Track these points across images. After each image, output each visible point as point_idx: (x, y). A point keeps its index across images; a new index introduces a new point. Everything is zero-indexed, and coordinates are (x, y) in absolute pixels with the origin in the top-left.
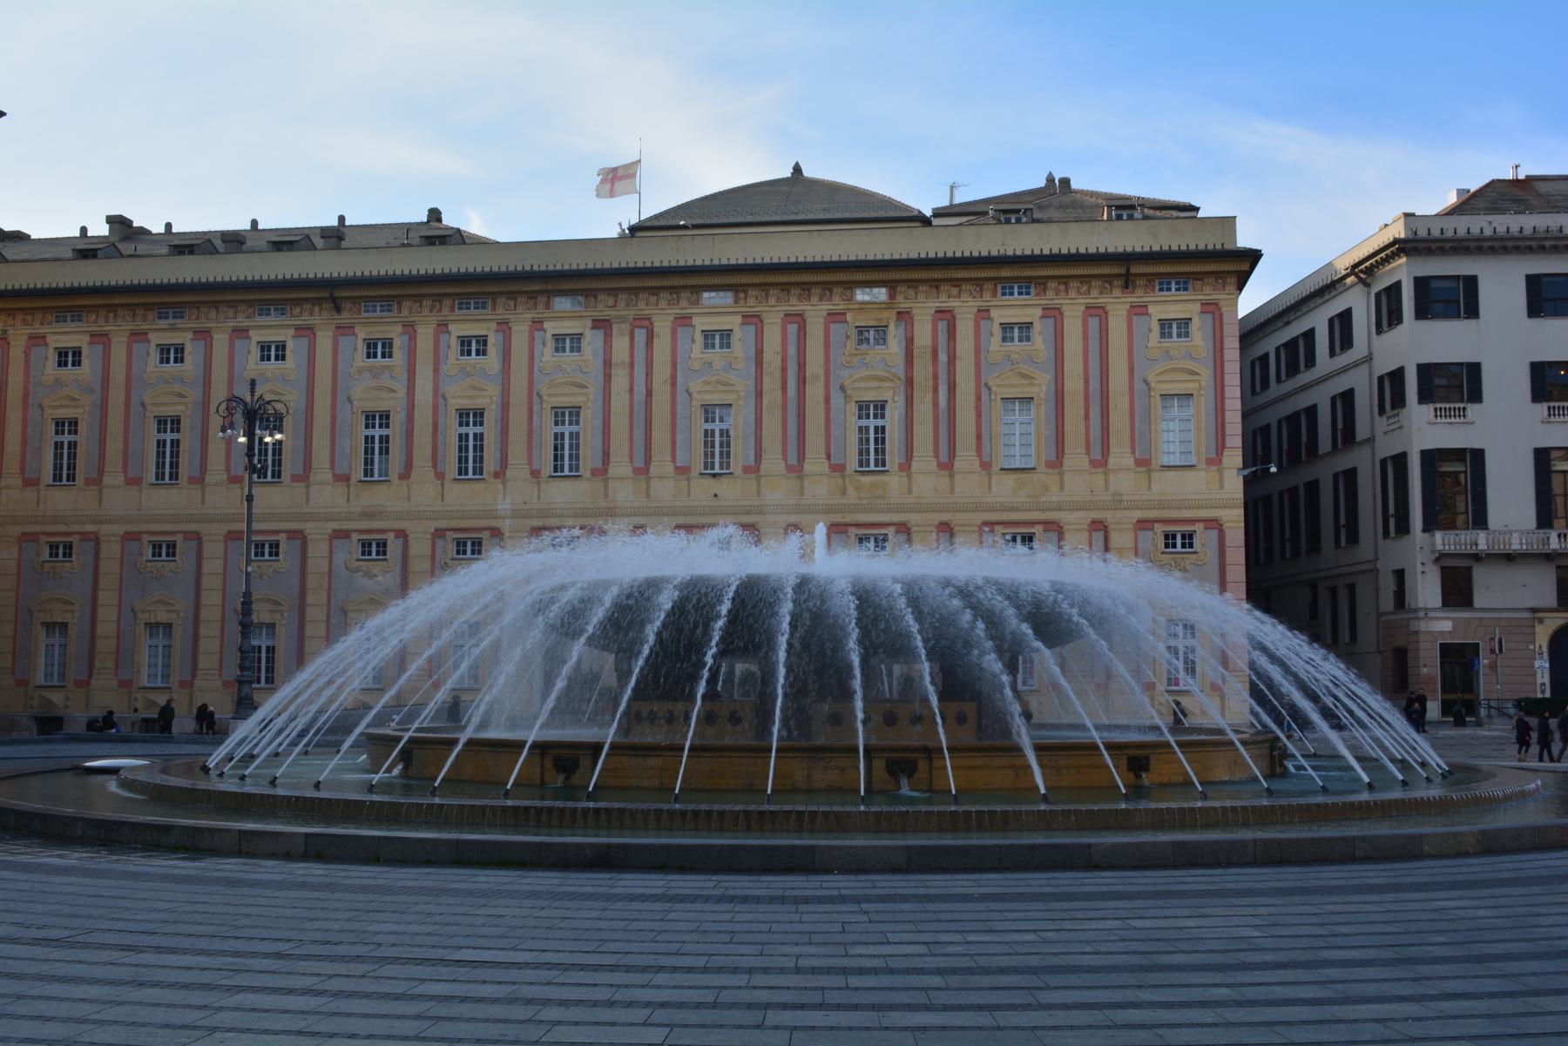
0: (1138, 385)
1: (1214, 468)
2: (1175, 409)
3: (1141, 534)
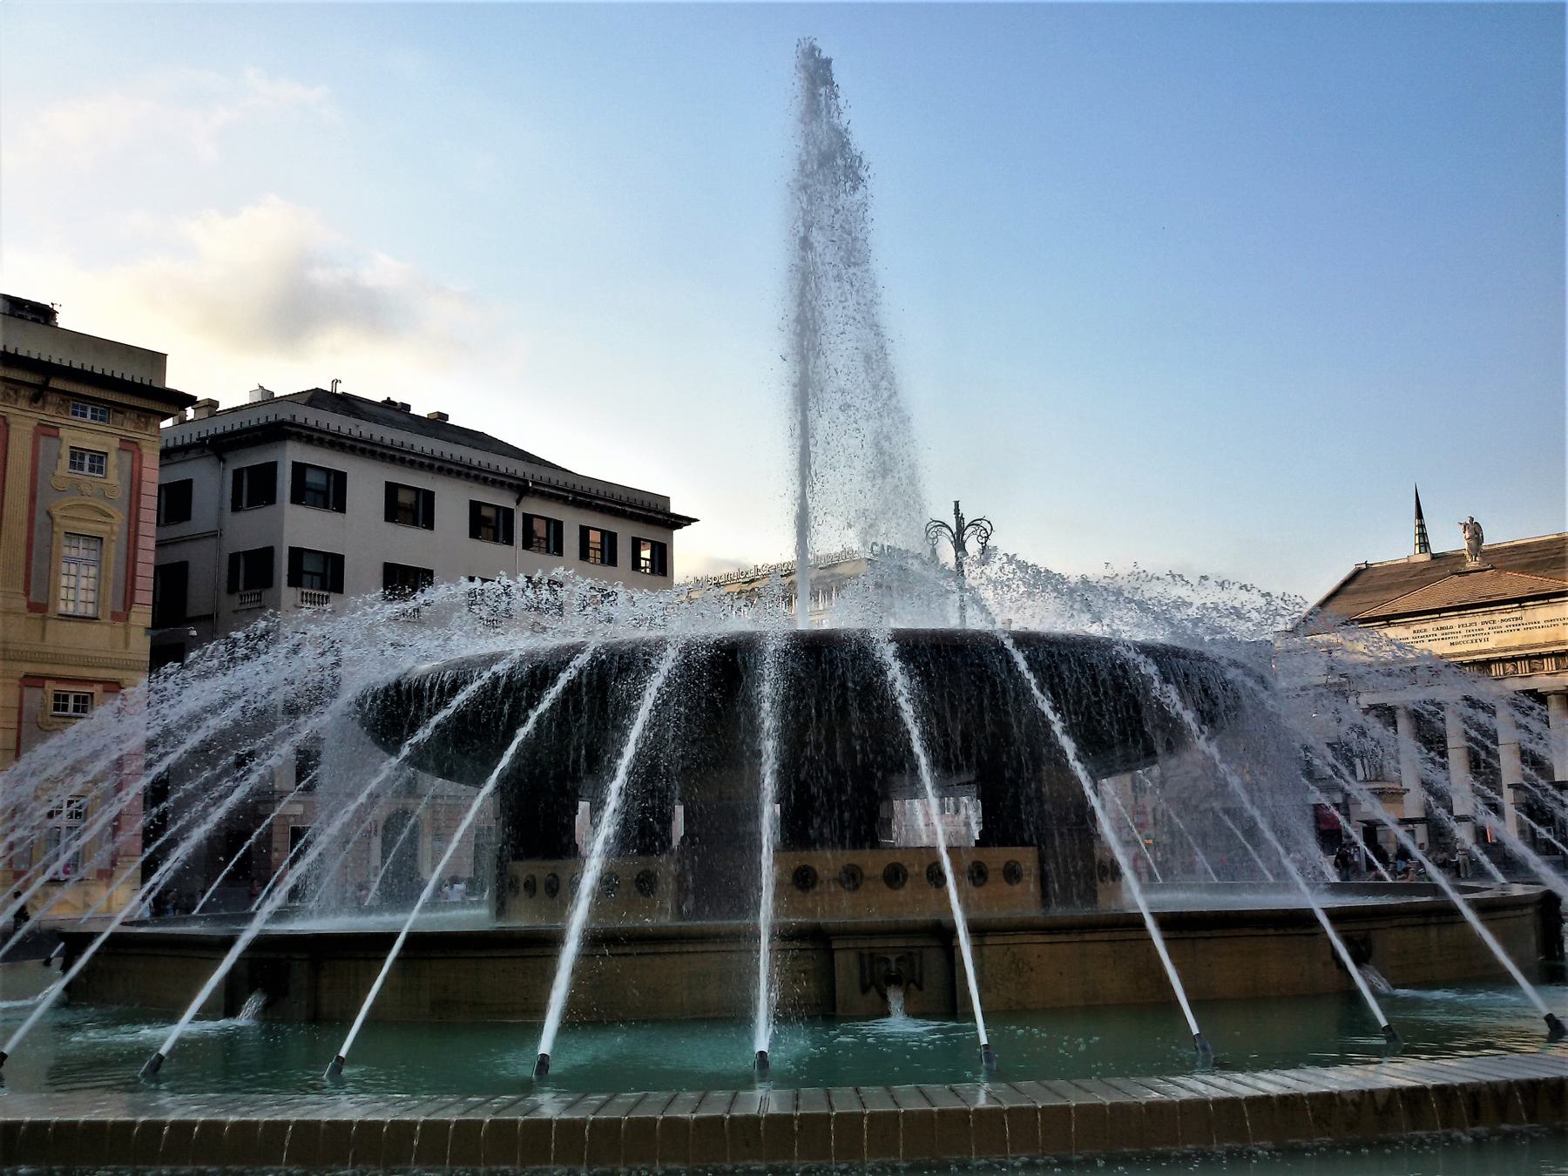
0: (40, 518)
2: (80, 551)
3: (27, 691)
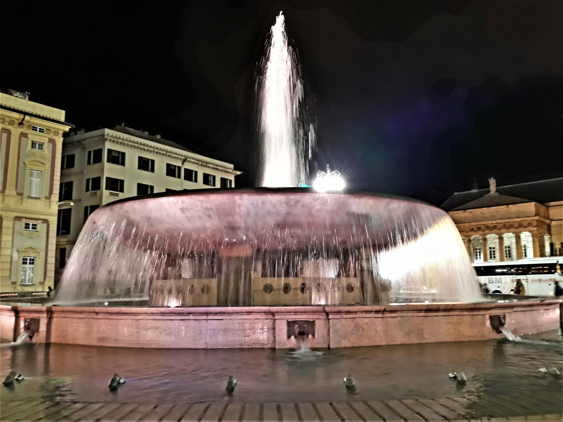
1: (47, 200)
3: (16, 222)
